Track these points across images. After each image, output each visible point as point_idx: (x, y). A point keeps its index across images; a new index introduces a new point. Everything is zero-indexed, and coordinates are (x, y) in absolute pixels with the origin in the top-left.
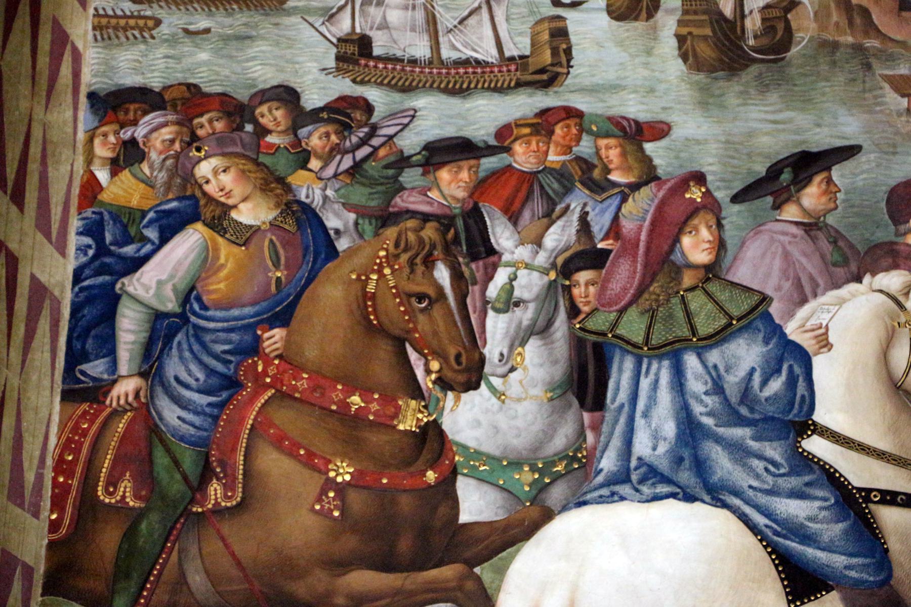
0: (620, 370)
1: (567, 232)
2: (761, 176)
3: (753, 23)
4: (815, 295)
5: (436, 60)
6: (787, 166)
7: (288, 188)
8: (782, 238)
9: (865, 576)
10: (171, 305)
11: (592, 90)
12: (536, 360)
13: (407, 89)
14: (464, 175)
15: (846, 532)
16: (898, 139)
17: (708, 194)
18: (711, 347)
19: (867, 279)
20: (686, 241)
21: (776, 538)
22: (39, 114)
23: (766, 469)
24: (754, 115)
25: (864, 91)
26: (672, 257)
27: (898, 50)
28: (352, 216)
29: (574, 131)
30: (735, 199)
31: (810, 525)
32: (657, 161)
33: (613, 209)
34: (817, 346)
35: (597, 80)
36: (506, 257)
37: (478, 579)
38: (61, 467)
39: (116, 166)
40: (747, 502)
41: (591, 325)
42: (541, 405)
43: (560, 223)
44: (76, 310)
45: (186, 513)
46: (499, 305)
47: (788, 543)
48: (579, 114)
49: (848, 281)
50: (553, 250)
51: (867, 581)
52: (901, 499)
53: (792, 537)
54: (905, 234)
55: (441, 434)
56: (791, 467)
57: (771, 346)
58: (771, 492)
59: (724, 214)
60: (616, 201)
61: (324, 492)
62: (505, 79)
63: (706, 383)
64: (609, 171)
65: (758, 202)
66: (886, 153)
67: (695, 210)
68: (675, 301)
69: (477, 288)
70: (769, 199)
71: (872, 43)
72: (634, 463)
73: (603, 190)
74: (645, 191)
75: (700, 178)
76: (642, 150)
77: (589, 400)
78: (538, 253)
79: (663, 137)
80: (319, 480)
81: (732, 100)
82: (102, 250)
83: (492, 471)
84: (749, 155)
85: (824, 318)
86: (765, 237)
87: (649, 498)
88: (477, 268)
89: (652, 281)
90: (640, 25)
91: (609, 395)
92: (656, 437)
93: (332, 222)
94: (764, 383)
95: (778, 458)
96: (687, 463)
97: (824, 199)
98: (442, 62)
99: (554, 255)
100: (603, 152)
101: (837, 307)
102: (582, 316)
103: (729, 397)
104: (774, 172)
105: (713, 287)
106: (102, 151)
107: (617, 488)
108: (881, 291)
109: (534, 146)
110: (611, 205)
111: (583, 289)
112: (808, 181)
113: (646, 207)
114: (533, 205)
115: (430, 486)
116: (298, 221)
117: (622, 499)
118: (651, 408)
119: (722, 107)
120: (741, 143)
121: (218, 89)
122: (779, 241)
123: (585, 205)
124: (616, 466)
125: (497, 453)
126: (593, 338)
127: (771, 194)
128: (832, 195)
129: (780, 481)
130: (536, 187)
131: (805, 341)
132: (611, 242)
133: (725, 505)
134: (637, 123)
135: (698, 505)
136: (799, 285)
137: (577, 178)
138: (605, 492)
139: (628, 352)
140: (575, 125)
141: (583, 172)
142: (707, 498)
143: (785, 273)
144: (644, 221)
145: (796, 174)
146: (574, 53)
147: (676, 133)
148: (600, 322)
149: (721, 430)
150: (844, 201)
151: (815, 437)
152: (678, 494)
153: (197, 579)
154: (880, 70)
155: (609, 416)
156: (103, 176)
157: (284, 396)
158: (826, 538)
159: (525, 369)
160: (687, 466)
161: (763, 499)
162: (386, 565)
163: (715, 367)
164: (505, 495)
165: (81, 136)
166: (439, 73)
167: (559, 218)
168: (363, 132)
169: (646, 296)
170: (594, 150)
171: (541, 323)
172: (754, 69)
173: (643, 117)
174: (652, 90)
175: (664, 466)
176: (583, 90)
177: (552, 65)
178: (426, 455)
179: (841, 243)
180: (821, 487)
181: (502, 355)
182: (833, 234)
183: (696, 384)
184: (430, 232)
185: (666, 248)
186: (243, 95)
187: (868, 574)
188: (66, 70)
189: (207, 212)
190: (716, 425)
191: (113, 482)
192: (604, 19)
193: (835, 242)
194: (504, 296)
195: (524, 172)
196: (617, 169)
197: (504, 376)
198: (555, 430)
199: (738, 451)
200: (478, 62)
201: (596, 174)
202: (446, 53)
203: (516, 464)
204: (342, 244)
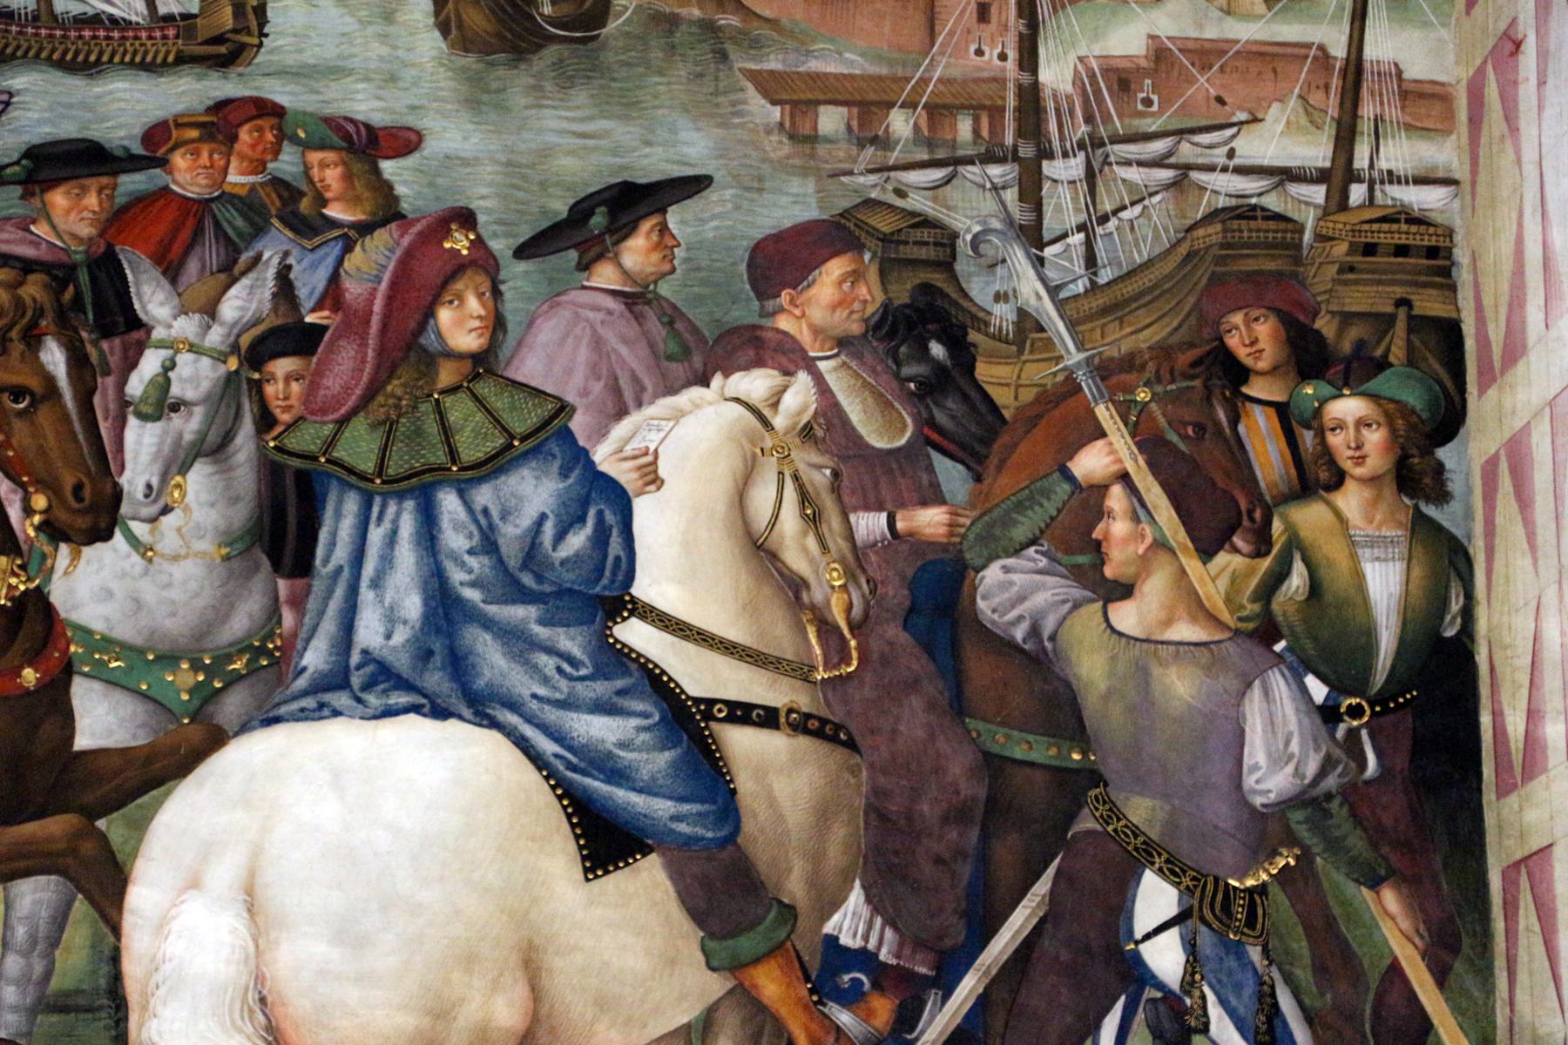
0: (338, 515)
1: (257, 297)
2: (558, 219)
4: (639, 405)
6: (598, 205)
8: (591, 315)
9: (700, 831)
12: (204, 497)
14: (92, 200)
15: (674, 765)
16: (765, 167)
17: (479, 243)
18: (481, 480)
19: (717, 380)
20: (445, 315)
21: (569, 774)
23: (559, 670)
24: (553, 124)
25: (716, 93)
26: (422, 341)
27: (767, 32)
29: (269, 137)
30: (523, 252)
31: (622, 753)
32: (400, 190)
33: (330, 262)
34: (640, 482)
35: (309, 57)
36: (158, 333)
37: (103, 838)
40: (529, 720)
41: (292, 442)
42: (210, 568)
43: (245, 282)
46: (146, 409)
47: (588, 781)
48: (278, 111)
49: (689, 384)
50: (235, 324)
51: (703, 839)
52: (758, 715)
53: (595, 773)
54: (774, 314)
55: (48, 610)
56: (597, 667)
57: (571, 481)
58: (565, 705)
59: (503, 275)
60: (335, 250)
62: (155, 50)
63: (470, 536)
64: (324, 202)
65: (554, 259)
66: (748, 189)
67: (458, 268)
68: (426, 407)
69: (110, 381)
70: (573, 255)
72: (355, 658)
73: (315, 232)
74: (381, 237)
75: (466, 218)
76: (377, 171)
77: (288, 559)
78: (210, 327)
79: (410, 152)
81: (518, 98)
83: (130, 669)
84: (543, 185)
85: (652, 440)
86: (566, 313)
87: (378, 713)
88: (112, 348)
89: (392, 373)
91: (320, 552)
92: (392, 619)
94: (560, 537)
95: (577, 652)
96: (437, 660)
97: (655, 257)
98: (54, 17)
99: (235, 331)
100: (315, 173)
101: (671, 424)
102: (279, 429)
103: (505, 559)
104: (581, 211)
105: (485, 388)
107: (327, 697)
108: (737, 400)
109: (204, 158)
110: (327, 255)
111: (281, 385)
112: (629, 230)
113: (382, 261)
114: (204, 252)
115: (28, 692)
117: (336, 713)
118: (385, 574)
119: (502, 108)
120: (532, 166)
122: (587, 320)
123: (286, 254)
124: (327, 662)
125: (138, 641)
126: (296, 463)
127: (575, 246)
128: (668, 252)
129: (579, 686)
130: (208, 223)
131: (623, 473)
132: (326, 313)
133: (494, 724)
134: (368, 127)
135: (453, 725)
136: (617, 391)
137: (274, 212)
138: (309, 702)
139: (352, 486)
140: (272, 128)
141: (284, 202)
142: (467, 713)
143: (594, 371)
144: (379, 283)
145: (613, 215)
146: (269, 14)
147: (431, 147)
148: (307, 438)
149: (493, 610)
150: (686, 260)
151: (634, 621)
152: (423, 706)
154: (742, 62)
155: (318, 586)
158: (644, 774)
159: (187, 509)
160: (439, 664)
161: (552, 715)
163: (486, 511)
164: (151, 706)
166: (51, 36)
167: (244, 273)
169: (380, 399)
170: (302, 168)
171: (213, 438)
172: (551, 52)
173: (379, 119)
174: (393, 78)
175: (402, 663)
176: (283, 73)
177: (235, 31)
179: (679, 326)
180: (641, 696)
181: (149, 487)
182: (669, 311)
183: (456, 539)
184: (33, 289)
185: (412, 325)
187: (705, 827)
190: (484, 602)
193: (671, 324)
194: (154, 396)
195: (188, 199)
196: (337, 199)
197: (153, 520)
198: (232, 606)
199: (518, 642)
200: (114, 21)
201: (305, 205)
203: (169, 659)
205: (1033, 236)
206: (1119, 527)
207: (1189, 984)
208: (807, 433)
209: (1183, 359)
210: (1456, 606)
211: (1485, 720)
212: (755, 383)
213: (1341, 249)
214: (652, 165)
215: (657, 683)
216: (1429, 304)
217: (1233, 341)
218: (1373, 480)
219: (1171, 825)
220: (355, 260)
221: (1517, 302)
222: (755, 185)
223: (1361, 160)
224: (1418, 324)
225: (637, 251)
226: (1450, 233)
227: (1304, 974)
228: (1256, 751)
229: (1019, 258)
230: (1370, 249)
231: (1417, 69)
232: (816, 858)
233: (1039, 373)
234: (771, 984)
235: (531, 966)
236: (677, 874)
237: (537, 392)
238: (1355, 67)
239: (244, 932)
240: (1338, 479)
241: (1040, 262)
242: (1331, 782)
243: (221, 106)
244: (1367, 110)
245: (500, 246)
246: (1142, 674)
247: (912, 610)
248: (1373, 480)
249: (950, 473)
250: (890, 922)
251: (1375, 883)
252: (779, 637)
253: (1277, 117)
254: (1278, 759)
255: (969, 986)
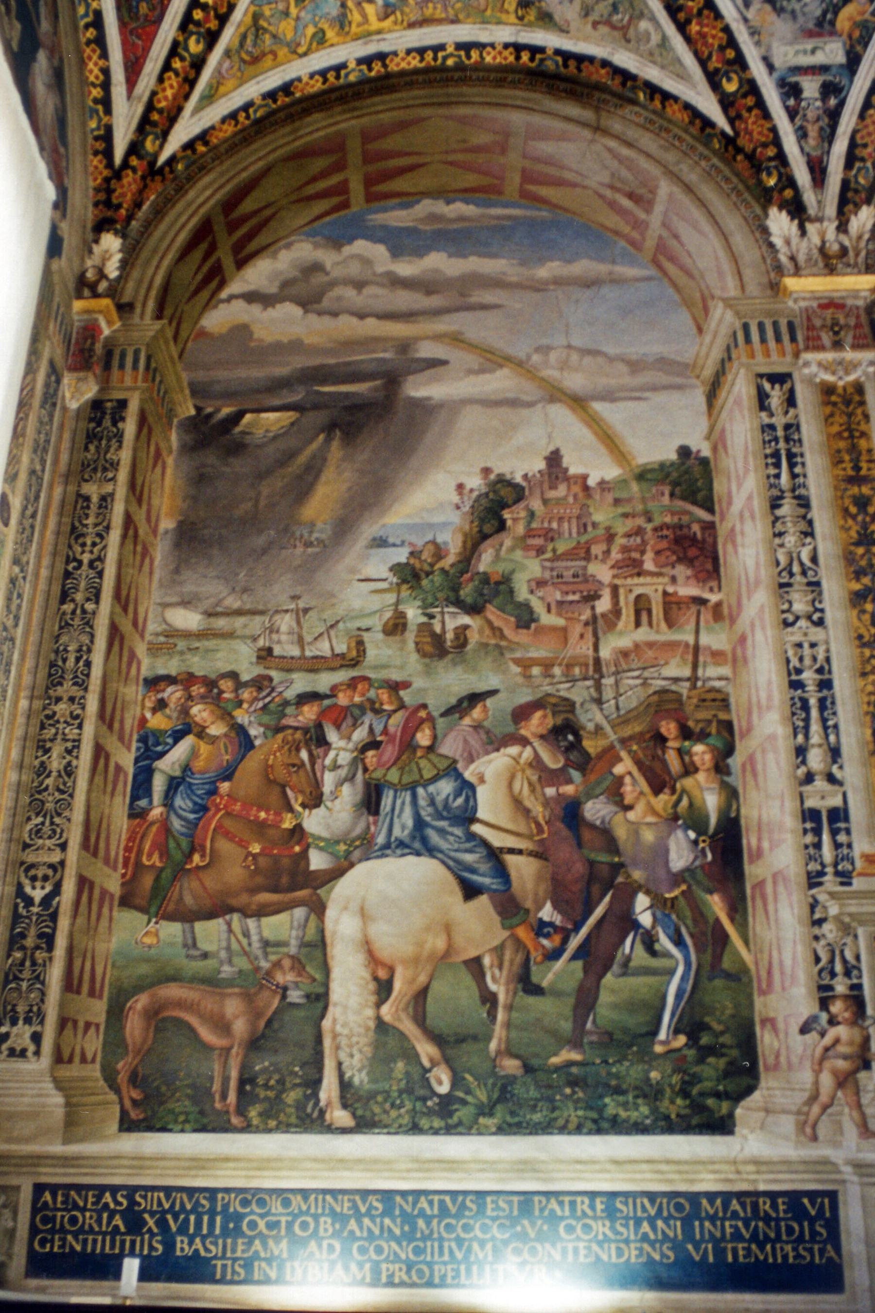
3: (450, 636)
5: (303, 657)
7: (232, 717)
10: (178, 773)
11: (375, 668)
13: (289, 670)
17: (429, 714)
19: (502, 750)
20: (419, 735)
22: (121, 689)
28: (262, 729)
30: (443, 715)
37: (318, 896)
38: (128, 849)
39: (154, 711)
41: (374, 775)
44: (135, 777)
45: (183, 869)
58: (456, 851)
61: (246, 857)
67: (422, 721)
71: (503, 643)
75: (424, 706)
80: (245, 852)
82: (147, 749)
85: (482, 769)
88: (320, 751)
90: (397, 638)
92: (403, 827)
93: (253, 732)
104: (460, 701)
105: (432, 756)
106: (149, 704)
116: (238, 734)
121: (201, 674)
143: (464, 750)
147: (415, 685)
148: (378, 774)
153: (188, 900)
154: (508, 655)
155: (381, 818)
156: (148, 715)
157: (228, 814)
161: (453, 854)
162: (275, 890)
165: (140, 698)
168: (268, 691)
172: (450, 656)
175: (407, 840)
178: (295, 839)
183: (422, 802)
184: (298, 735)
186: (213, 676)
188: (133, 671)
189: (196, 730)
191: (150, 856)
192: (380, 636)
199: (442, 832)
201: (377, 705)
202: (308, 653)
203: (337, 842)
204: (257, 743)
205: (599, 701)
206: (628, 788)
207: (653, 927)
208: (530, 765)
209: (648, 736)
210: (734, 807)
211: (744, 842)
212: (514, 750)
213: (695, 701)
214: (482, 687)
215: (485, 843)
216: (722, 716)
217: (663, 731)
218: (708, 770)
219: (647, 880)
220: (392, 721)
221: (750, 713)
222: (512, 690)
223: (700, 672)
224: (720, 722)
225: (477, 713)
226: (728, 694)
227: (689, 922)
228: (673, 855)
229: (594, 707)
230: (704, 700)
231: (715, 646)
232: (536, 894)
233: (602, 743)
234: (522, 932)
235: (448, 929)
236: (491, 898)
237: (446, 757)
238: (697, 648)
239: (360, 924)
240: (696, 770)
241: (601, 710)
242: (697, 863)
243: (353, 679)
244: (701, 659)
245: (436, 714)
246: (637, 833)
247: (565, 817)
248: (708, 770)
249: (575, 775)
250: (559, 912)
251: (711, 892)
252: (521, 827)
253: (674, 662)
254: (680, 857)
255: (584, 931)
